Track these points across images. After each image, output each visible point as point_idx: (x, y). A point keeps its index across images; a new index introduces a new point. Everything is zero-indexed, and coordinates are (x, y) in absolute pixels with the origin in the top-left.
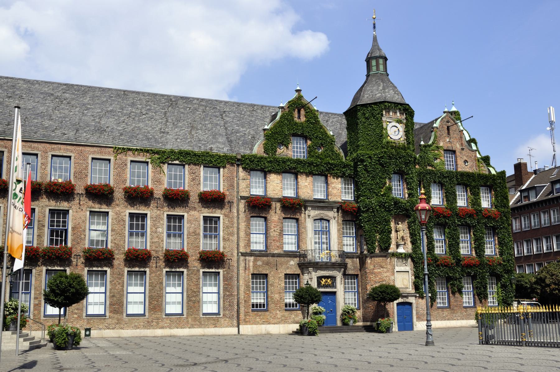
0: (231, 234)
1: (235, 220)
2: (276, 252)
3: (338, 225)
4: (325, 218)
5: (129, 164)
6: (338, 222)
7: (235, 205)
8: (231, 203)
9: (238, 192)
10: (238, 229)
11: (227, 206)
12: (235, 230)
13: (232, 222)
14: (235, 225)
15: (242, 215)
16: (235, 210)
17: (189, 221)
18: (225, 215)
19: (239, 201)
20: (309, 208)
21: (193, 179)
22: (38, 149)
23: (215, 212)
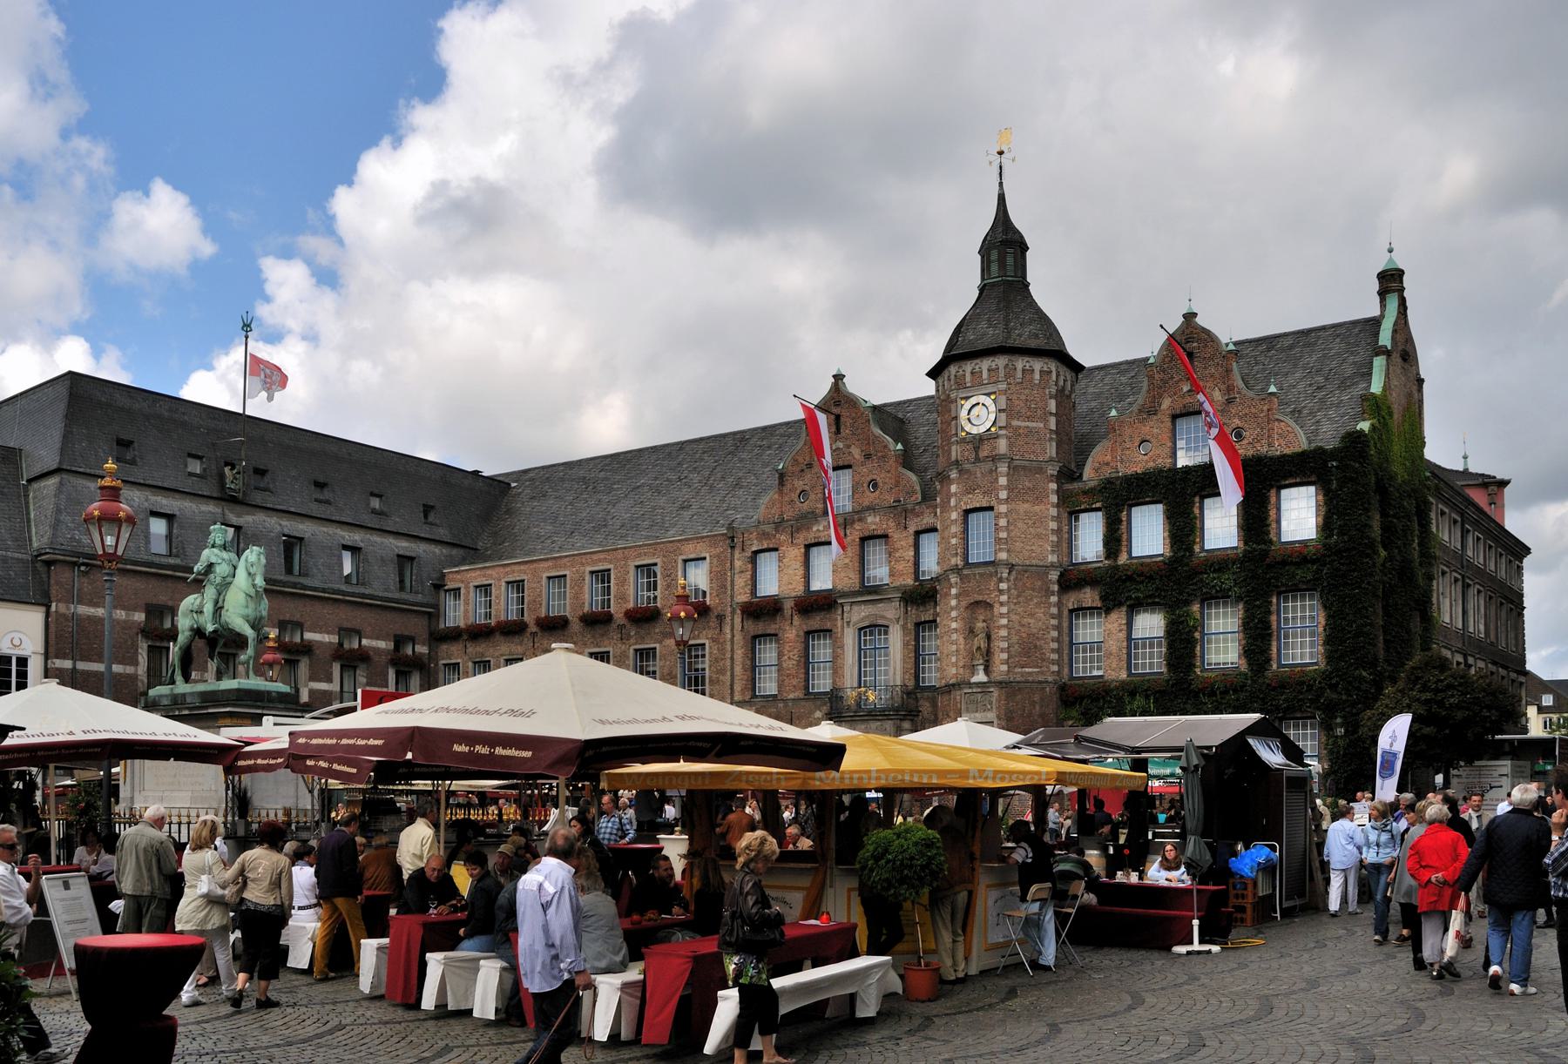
0: (722, 672)
1: (729, 648)
2: (791, 696)
3: (905, 635)
4: (880, 622)
5: (588, 578)
6: (904, 627)
7: (728, 619)
8: (721, 618)
9: (732, 597)
10: (732, 659)
11: (713, 622)
12: (728, 663)
13: (722, 650)
14: (728, 655)
15: (738, 637)
16: (727, 630)
17: (663, 657)
18: (713, 640)
19: (733, 612)
20: (847, 608)
21: (668, 586)
22: (490, 576)
23: (698, 637)
